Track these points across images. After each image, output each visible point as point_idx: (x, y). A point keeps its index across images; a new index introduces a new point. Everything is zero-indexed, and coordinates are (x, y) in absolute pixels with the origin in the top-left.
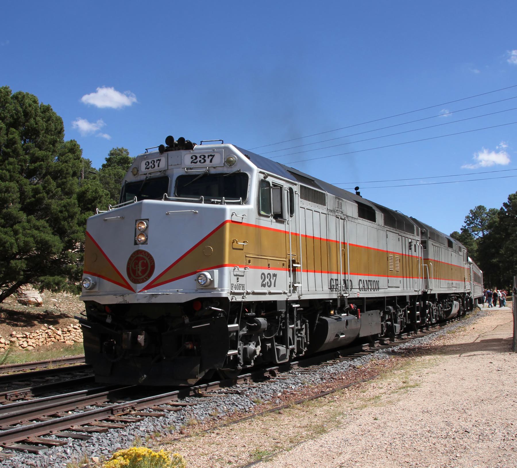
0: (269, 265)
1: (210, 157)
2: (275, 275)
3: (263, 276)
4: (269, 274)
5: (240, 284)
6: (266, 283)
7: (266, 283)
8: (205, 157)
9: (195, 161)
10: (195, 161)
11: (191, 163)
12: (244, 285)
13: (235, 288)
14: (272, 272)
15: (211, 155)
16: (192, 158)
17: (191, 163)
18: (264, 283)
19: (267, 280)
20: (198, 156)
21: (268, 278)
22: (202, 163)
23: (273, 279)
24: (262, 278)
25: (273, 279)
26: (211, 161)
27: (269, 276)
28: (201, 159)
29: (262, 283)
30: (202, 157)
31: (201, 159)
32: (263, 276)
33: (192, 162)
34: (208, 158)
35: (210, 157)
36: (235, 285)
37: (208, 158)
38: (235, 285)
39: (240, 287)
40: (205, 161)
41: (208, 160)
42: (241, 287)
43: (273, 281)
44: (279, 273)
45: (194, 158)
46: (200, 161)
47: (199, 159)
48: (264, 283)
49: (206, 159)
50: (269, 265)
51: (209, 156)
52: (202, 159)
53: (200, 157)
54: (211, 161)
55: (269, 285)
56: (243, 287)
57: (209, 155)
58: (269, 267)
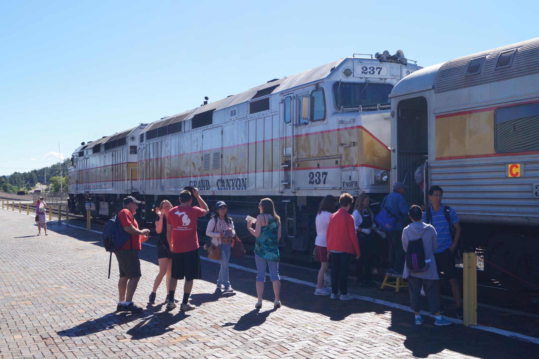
0: (318, 165)
1: (379, 70)
2: (325, 173)
3: (311, 175)
4: (319, 173)
5: (352, 182)
6: (314, 180)
7: (314, 180)
8: (374, 68)
9: (366, 72)
10: (366, 72)
11: (362, 73)
12: (357, 182)
13: (347, 185)
14: (321, 171)
15: (379, 68)
16: (363, 69)
17: (362, 73)
18: (312, 180)
19: (315, 178)
20: (368, 67)
21: (316, 176)
22: (371, 74)
23: (323, 177)
24: (310, 176)
25: (323, 177)
26: (379, 73)
27: (318, 174)
28: (370, 70)
29: (310, 181)
30: (372, 69)
31: (370, 70)
32: (311, 175)
33: (362, 73)
34: (377, 70)
35: (379, 70)
36: (347, 183)
37: (377, 70)
38: (347, 183)
39: (352, 184)
40: (374, 72)
41: (376, 72)
42: (354, 184)
43: (322, 179)
44: (330, 171)
45: (365, 69)
46: (370, 72)
47: (368, 70)
48: (312, 180)
49: (375, 70)
50: (318, 165)
51: (377, 68)
52: (372, 70)
53: (370, 69)
54: (379, 73)
55: (317, 182)
56: (355, 184)
57: (378, 67)
58: (318, 167)
